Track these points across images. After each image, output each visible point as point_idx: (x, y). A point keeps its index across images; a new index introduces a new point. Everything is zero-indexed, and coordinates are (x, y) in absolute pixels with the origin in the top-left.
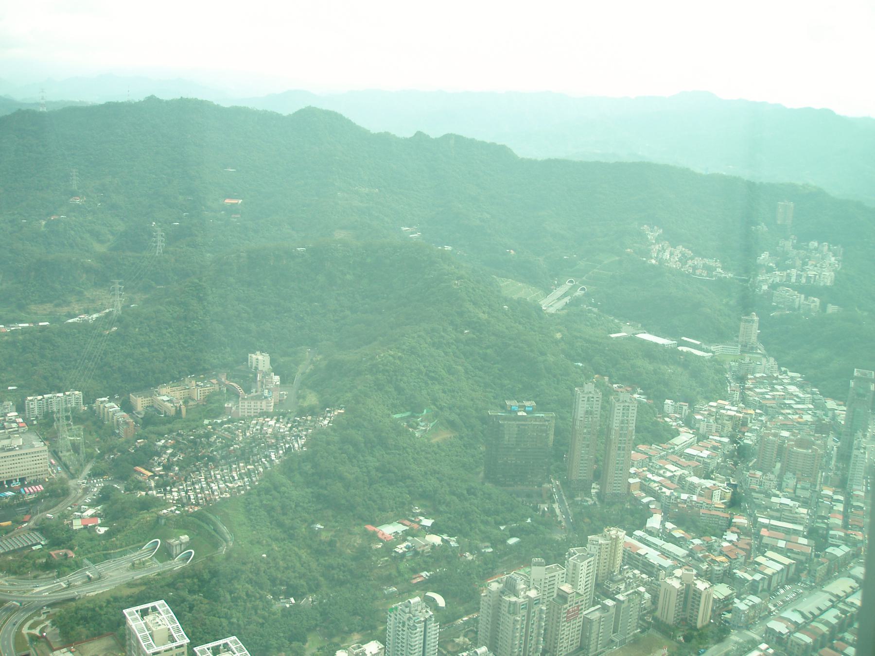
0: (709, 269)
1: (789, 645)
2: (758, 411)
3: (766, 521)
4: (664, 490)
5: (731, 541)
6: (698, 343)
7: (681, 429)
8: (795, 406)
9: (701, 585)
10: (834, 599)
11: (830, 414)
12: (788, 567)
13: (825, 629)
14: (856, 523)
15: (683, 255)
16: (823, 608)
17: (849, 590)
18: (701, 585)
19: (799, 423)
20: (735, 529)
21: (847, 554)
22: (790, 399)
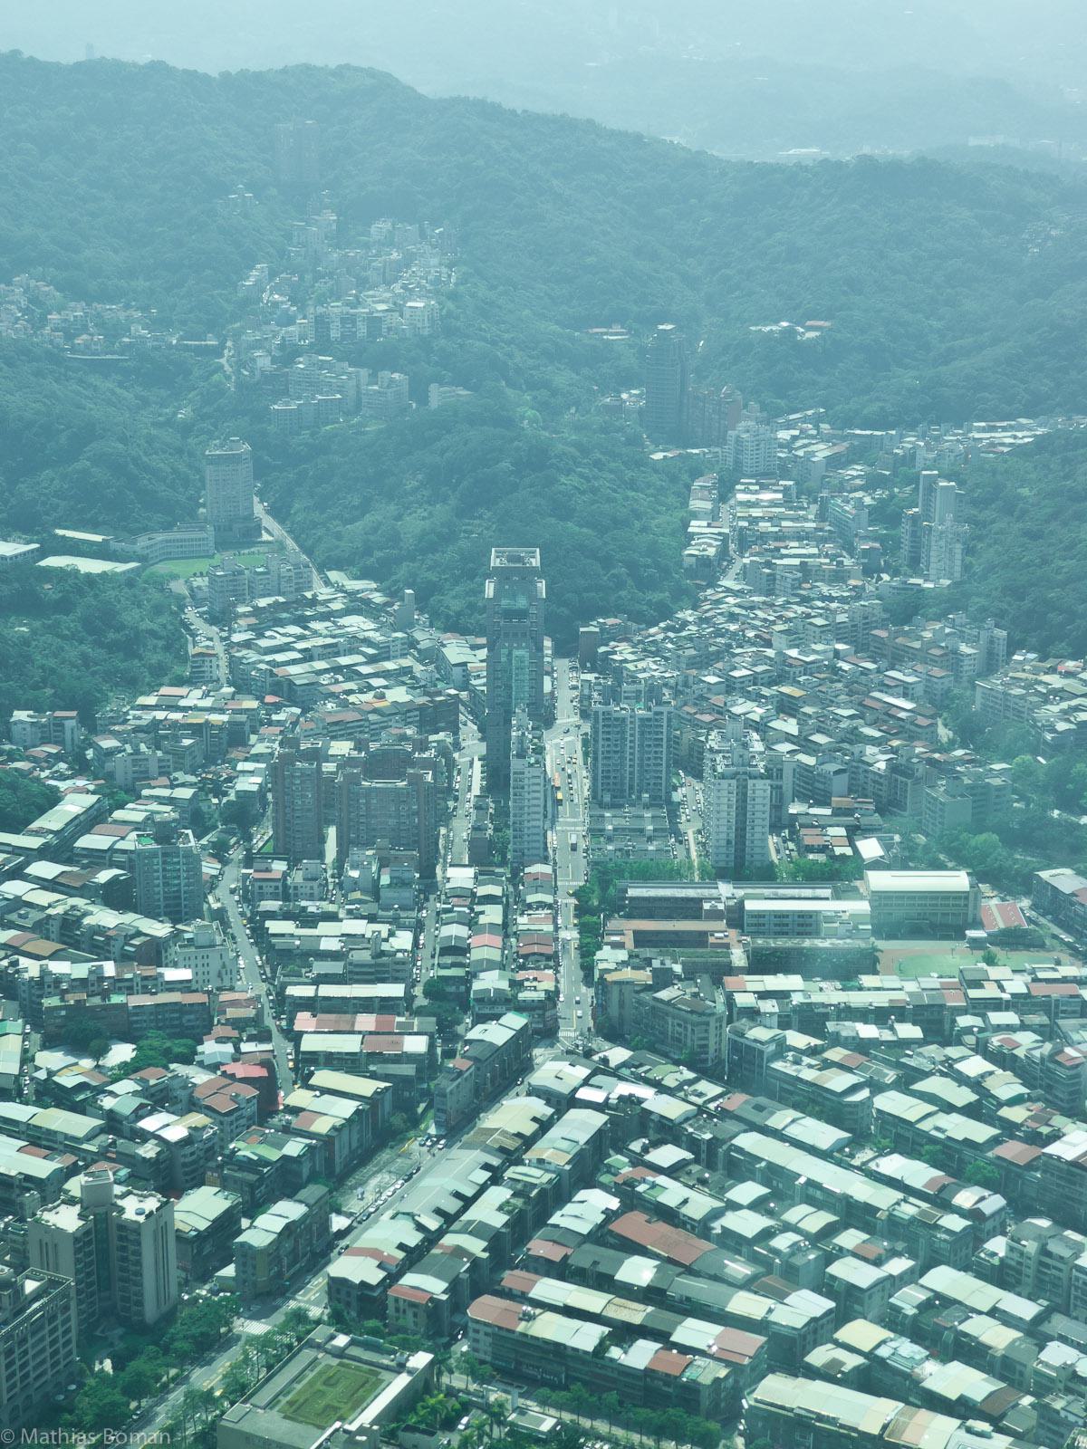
0: (113, 331)
1: (391, 1311)
2: (270, 699)
3: (308, 991)
4: (24, 962)
5: (214, 1067)
6: (99, 538)
7: (62, 785)
8: (365, 670)
9: (135, 1207)
10: (496, 1162)
11: (457, 672)
12: (374, 1101)
13: (477, 1247)
14: (536, 949)
15: (34, 300)
16: (469, 1192)
17: (529, 1129)
18: (135, 1207)
19: (375, 711)
20: (229, 1031)
21: (521, 1033)
22: (351, 651)
